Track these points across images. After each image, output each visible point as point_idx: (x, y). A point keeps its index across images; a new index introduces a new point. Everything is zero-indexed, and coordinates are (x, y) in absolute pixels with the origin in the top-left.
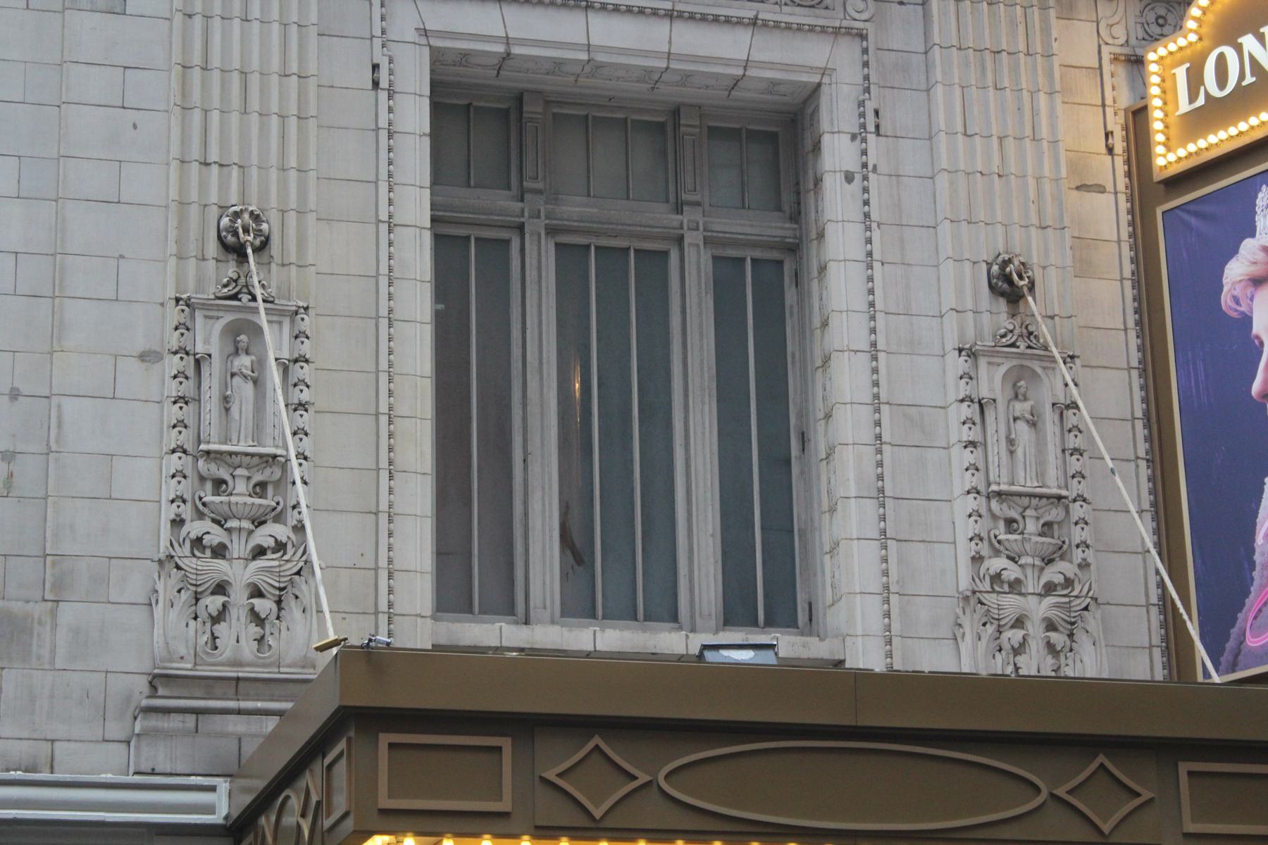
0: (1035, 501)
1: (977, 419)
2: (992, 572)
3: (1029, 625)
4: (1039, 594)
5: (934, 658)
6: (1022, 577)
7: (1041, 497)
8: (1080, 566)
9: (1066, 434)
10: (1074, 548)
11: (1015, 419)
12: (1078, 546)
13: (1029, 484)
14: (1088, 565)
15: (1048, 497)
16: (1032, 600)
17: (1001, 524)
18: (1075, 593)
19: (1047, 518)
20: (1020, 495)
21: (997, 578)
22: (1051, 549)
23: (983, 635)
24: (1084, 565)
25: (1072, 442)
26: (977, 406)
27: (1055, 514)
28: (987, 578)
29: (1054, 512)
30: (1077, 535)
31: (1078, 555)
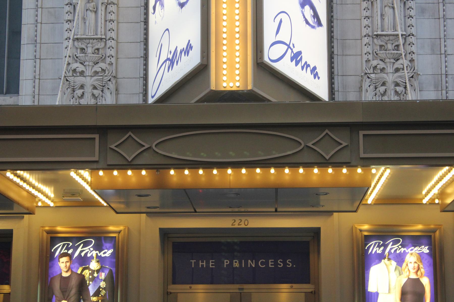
0: (91, 41)
1: (72, 11)
2: (73, 69)
3: (85, 88)
4: (91, 76)
5: (47, 101)
6: (84, 70)
7: (94, 39)
8: (109, 64)
9: (108, 14)
10: (107, 58)
11: (87, 10)
12: (109, 57)
13: (89, 35)
14: (112, 64)
15: (97, 39)
16: (88, 78)
17: (79, 50)
18: (105, 75)
19: (97, 47)
20: (86, 39)
21: (74, 71)
22: (97, 58)
23: (66, 92)
24: (111, 64)
25: (109, 17)
26: (73, 6)
27: (100, 45)
28: (71, 71)
29: (99, 44)
30: (109, 52)
31: (108, 60)
